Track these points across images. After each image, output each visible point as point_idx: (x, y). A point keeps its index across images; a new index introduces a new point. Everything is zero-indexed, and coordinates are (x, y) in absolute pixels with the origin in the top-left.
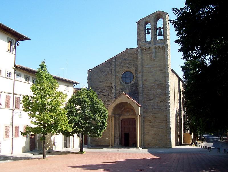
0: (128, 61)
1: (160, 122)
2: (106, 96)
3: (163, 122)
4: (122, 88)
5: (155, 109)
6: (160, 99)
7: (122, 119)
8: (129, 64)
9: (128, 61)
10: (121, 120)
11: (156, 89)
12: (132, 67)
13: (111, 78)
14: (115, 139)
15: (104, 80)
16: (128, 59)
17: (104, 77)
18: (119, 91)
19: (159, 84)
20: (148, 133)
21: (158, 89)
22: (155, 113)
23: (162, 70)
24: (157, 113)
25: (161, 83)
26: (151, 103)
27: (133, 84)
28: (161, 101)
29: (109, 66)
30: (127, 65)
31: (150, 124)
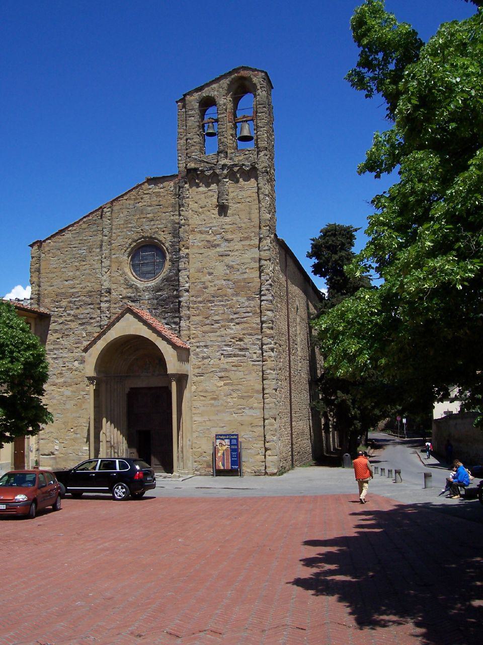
0: (148, 216)
1: (242, 397)
2: (84, 321)
3: (252, 397)
4: (129, 295)
5: (230, 356)
6: (242, 326)
7: (131, 389)
8: (152, 223)
9: (148, 216)
10: (127, 392)
11: (233, 295)
12: (160, 232)
13: (98, 266)
14: (107, 449)
15: (78, 273)
16: (150, 208)
17: (77, 264)
18: (121, 304)
19: (239, 281)
20: (208, 429)
21: (237, 295)
22: (226, 370)
23: (247, 238)
24: (234, 368)
25: (246, 276)
26: (219, 339)
27: (163, 280)
28: (245, 332)
29: (92, 230)
30: (147, 228)
31: (212, 402)
